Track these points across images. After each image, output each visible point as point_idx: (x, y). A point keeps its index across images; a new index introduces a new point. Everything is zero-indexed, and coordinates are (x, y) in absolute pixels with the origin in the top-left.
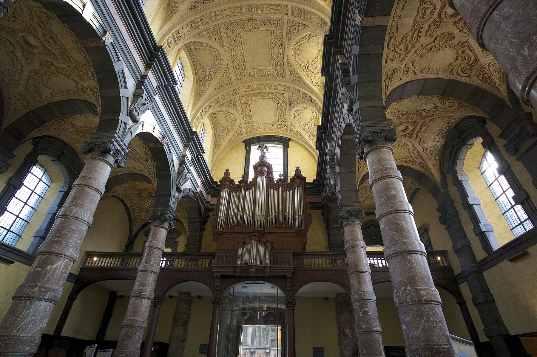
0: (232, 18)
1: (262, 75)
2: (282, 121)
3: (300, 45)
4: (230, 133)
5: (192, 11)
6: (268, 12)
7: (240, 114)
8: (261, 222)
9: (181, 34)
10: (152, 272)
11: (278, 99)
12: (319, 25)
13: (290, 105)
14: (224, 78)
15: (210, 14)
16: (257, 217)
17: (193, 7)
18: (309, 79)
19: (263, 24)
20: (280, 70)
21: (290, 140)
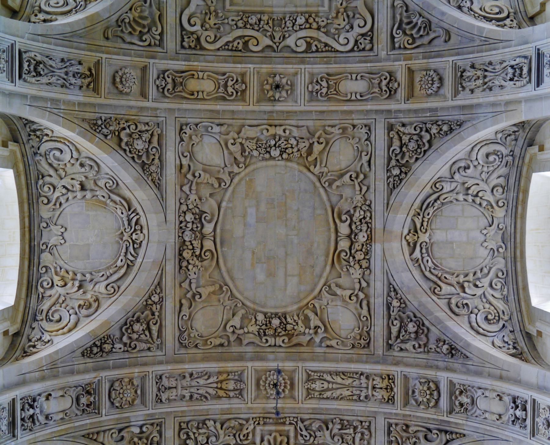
0: (210, 403)
5: (89, 360)
6: (328, 394)
9: (38, 411)
12: (505, 418)
15: (143, 378)
17: (95, 350)
19: (304, 433)
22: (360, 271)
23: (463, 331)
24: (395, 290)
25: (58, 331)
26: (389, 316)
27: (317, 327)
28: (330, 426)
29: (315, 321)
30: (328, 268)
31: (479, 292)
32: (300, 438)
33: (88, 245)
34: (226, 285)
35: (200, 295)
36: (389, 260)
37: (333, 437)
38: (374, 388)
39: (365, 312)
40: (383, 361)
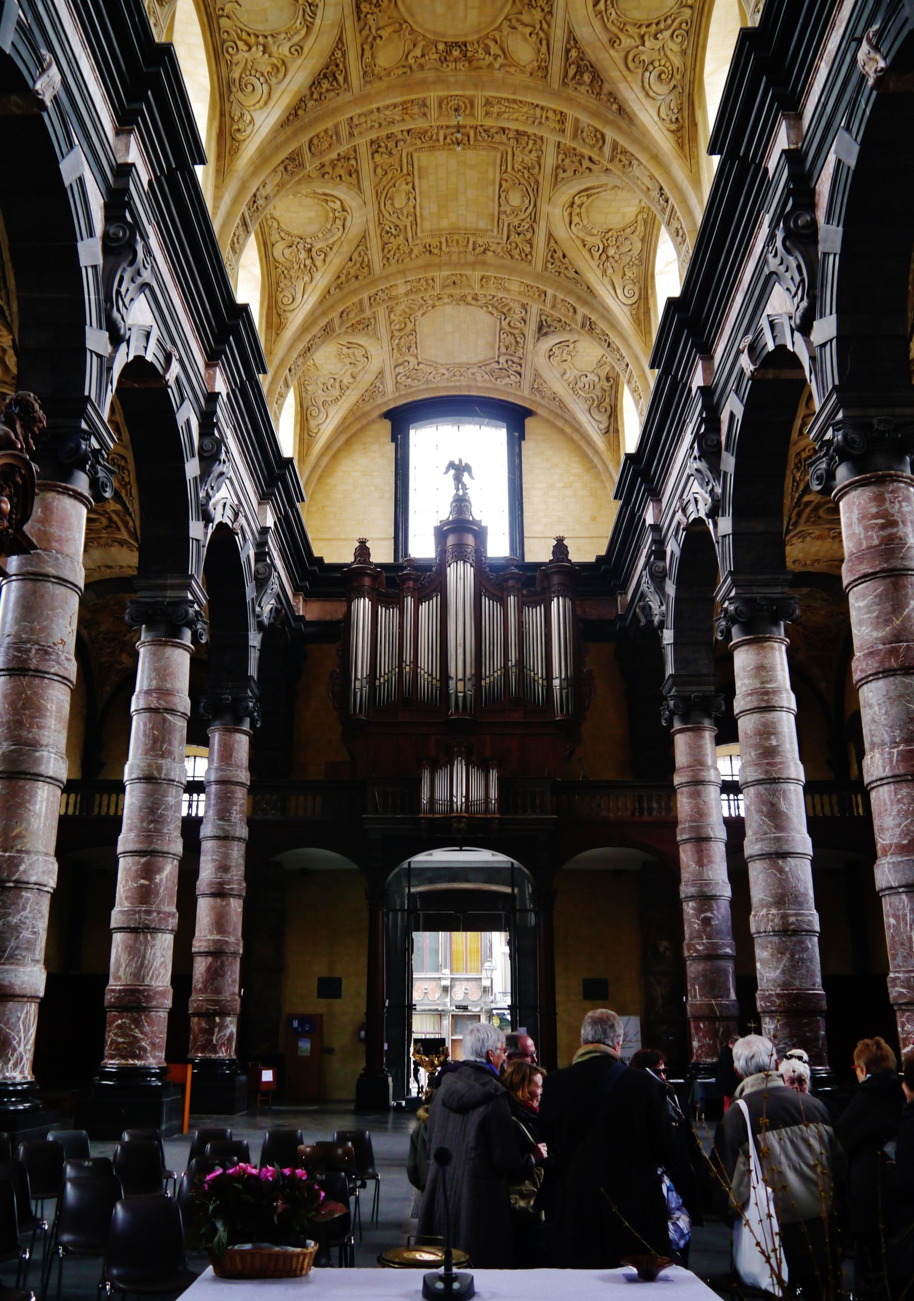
1: (462, 249)
2: (510, 363)
3: (588, 196)
4: (347, 393)
6: (506, 116)
7: (385, 343)
8: (465, 697)
10: (234, 838)
11: (505, 310)
13: (540, 329)
14: (350, 264)
16: (452, 683)
18: (606, 281)
19: (483, 134)
20: (520, 244)
21: (528, 413)
22: (542, 14)
23: (633, 96)
24: (574, 39)
25: (254, 105)
26: (567, 59)
27: (496, 57)
28: (507, 132)
29: (494, 49)
30: (509, 6)
31: (658, 44)
32: (479, 138)
33: (265, 10)
34: (405, 21)
35: (381, 37)
36: (571, 13)
37: (509, 139)
38: (547, 118)
39: (544, 49)
40: (557, 95)
